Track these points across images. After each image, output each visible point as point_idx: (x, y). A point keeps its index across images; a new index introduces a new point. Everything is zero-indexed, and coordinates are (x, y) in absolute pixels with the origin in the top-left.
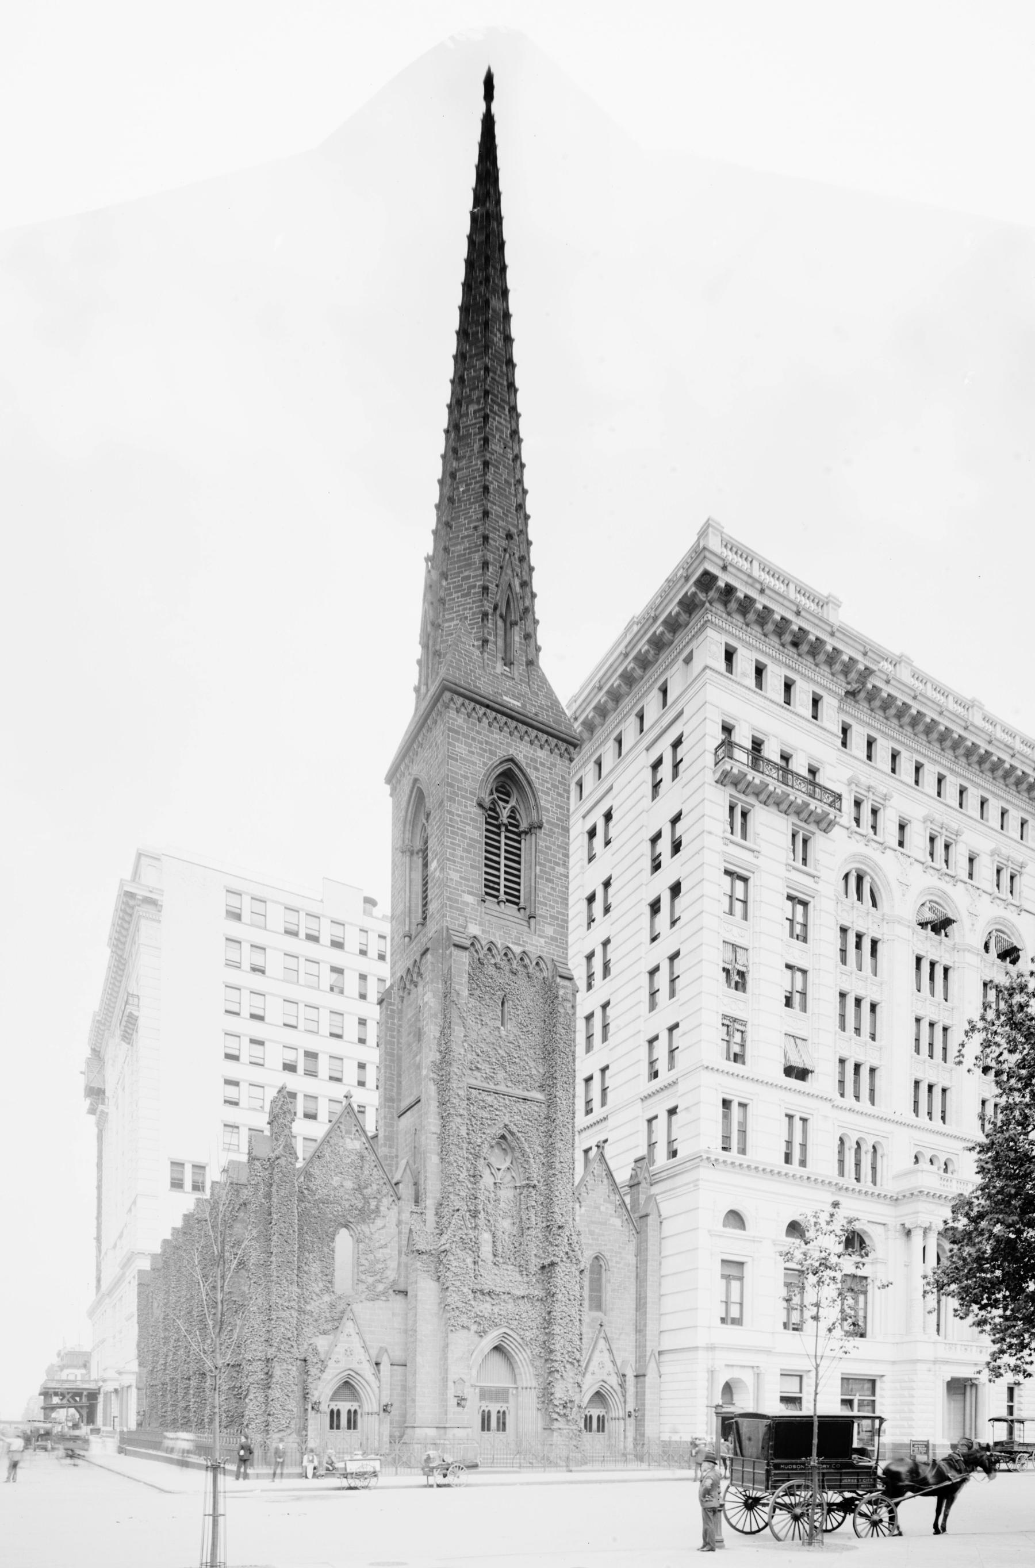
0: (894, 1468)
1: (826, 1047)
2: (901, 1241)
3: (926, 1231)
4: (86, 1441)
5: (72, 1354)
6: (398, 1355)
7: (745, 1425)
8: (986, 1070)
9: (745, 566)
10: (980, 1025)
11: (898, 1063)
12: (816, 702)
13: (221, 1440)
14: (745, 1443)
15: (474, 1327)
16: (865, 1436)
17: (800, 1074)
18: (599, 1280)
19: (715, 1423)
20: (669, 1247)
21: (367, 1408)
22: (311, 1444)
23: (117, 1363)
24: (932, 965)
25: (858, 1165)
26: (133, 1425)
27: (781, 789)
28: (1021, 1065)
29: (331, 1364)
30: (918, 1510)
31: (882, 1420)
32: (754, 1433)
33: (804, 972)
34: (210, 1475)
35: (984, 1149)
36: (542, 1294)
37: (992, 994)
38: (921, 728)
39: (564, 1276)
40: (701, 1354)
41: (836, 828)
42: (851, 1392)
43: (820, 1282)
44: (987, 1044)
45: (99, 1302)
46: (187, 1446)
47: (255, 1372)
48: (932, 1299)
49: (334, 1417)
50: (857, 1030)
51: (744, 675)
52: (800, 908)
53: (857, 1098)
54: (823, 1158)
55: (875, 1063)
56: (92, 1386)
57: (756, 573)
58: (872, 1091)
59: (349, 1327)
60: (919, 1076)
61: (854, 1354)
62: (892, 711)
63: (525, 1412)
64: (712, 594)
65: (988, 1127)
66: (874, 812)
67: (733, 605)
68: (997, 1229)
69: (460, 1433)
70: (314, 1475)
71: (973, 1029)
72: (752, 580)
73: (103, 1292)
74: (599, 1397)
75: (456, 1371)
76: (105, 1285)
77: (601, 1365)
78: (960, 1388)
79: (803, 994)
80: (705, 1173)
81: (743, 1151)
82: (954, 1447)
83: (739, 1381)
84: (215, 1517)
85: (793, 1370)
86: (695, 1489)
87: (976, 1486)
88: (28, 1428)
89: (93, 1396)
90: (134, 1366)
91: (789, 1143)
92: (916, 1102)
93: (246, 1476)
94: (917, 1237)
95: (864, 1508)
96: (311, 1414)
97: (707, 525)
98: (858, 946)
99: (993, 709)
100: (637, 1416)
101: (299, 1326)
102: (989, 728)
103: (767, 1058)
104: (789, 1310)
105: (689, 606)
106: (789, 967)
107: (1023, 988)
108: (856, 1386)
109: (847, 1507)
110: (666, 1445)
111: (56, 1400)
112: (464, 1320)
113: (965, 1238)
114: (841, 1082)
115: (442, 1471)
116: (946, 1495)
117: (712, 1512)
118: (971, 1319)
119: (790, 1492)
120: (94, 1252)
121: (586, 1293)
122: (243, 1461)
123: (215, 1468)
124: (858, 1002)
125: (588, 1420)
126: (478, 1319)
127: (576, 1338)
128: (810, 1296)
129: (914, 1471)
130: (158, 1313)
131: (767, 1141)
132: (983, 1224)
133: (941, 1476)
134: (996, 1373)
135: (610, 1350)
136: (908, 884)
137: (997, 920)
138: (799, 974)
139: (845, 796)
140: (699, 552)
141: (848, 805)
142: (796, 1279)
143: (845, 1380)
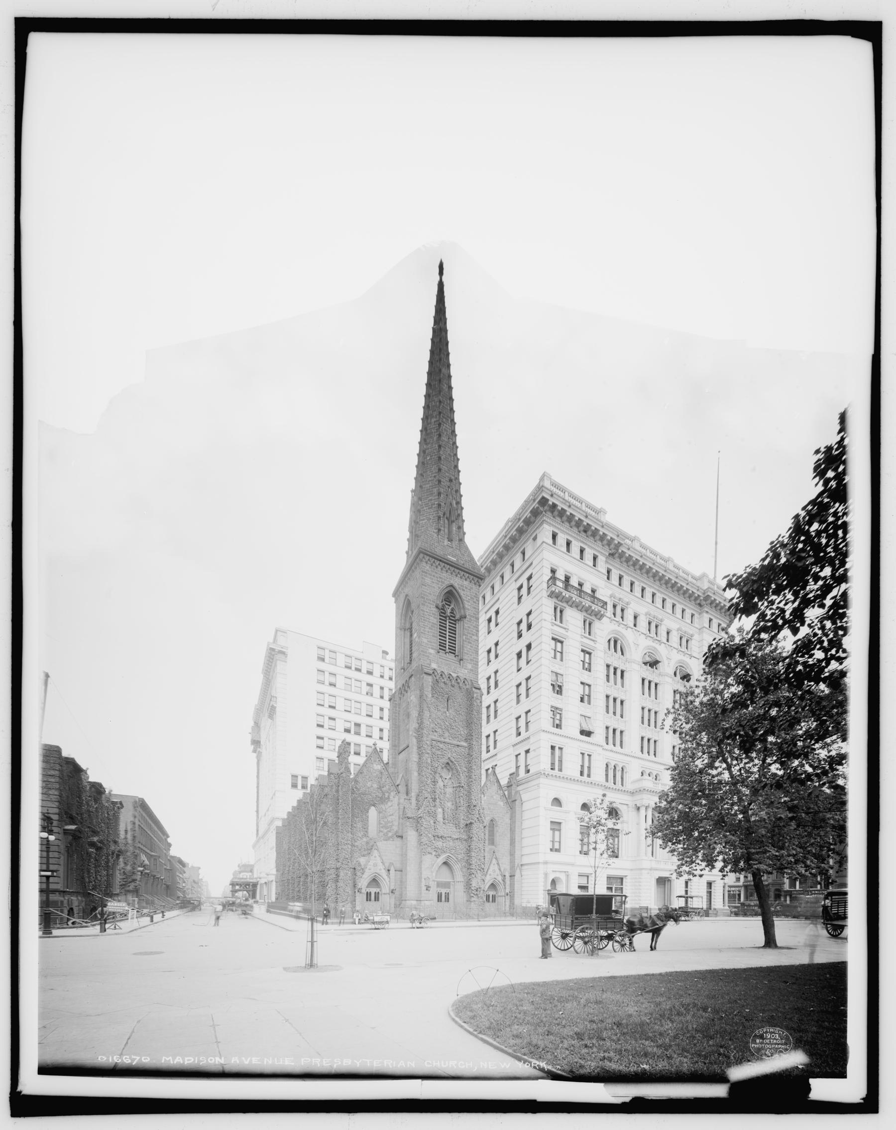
0: (631, 919)
1: (599, 721)
2: (635, 813)
3: (647, 808)
4: (252, 907)
5: (245, 866)
6: (398, 866)
7: (561, 899)
8: (675, 732)
9: (578, 505)
10: (672, 710)
11: (634, 729)
12: (595, 558)
13: (315, 906)
14: (562, 907)
15: (434, 853)
16: (618, 904)
17: (587, 733)
18: (493, 831)
19: (547, 898)
20: (526, 815)
21: (384, 891)
22: (358, 908)
23: (266, 870)
24: (650, 682)
25: (615, 776)
26: (274, 899)
27: (578, 599)
28: (692, 729)
29: (367, 870)
30: (642, 939)
31: (626, 897)
32: (566, 903)
33: (589, 686)
34: (310, 923)
35: (674, 769)
36: (466, 837)
37: (678, 696)
38: (644, 571)
39: (476, 829)
40: (541, 866)
41: (605, 618)
42: (611, 884)
43: (597, 832)
44: (675, 720)
45: (258, 841)
46: (299, 909)
47: (331, 874)
48: (649, 840)
49: (368, 895)
50: (614, 713)
51: (561, 546)
52: (587, 656)
53: (614, 745)
54: (598, 774)
55: (623, 729)
56: (254, 881)
57: (567, 498)
58: (621, 742)
59: (375, 853)
60: (644, 735)
61: (613, 866)
62: (631, 563)
63: (458, 893)
64: (546, 508)
65: (676, 759)
66: (622, 610)
67: (556, 513)
68: (680, 807)
69: (427, 903)
70: (359, 923)
71: (669, 712)
72: (565, 501)
73: (260, 837)
74: (493, 886)
75: (425, 873)
76: (260, 834)
77: (494, 871)
78: (662, 882)
79: (589, 696)
80: (543, 780)
81: (560, 770)
82: (660, 909)
83: (559, 878)
84: (312, 942)
85: (581, 871)
86: (538, 929)
87: (670, 929)
88: (224, 901)
89: (255, 885)
90: (274, 872)
91: (582, 766)
92: (642, 747)
93: (327, 923)
94: (643, 810)
95: (617, 938)
96: (357, 894)
97: (544, 475)
98: (615, 673)
99: (678, 561)
100: (511, 895)
101: (352, 852)
102: (677, 571)
103: (571, 726)
104: (582, 845)
105: (535, 513)
106: (582, 683)
107: (692, 693)
108: (614, 881)
109: (610, 937)
110: (525, 908)
111: (237, 887)
112: (429, 849)
113: (666, 811)
114: (607, 738)
115: (419, 921)
116: (656, 932)
117: (546, 941)
118: (668, 849)
119: (582, 931)
120: (255, 818)
121: (487, 837)
122: (326, 916)
123: (312, 920)
124: (615, 700)
125: (488, 897)
126: (436, 849)
127: (482, 858)
128: (592, 838)
129: (641, 921)
130: (286, 846)
131: (572, 766)
132: (674, 804)
133: (654, 923)
134: (680, 874)
135: (498, 864)
136: (638, 644)
137: (680, 661)
138: (587, 687)
139: (609, 602)
140: (540, 488)
141: (610, 607)
142: (585, 831)
143: (609, 878)
